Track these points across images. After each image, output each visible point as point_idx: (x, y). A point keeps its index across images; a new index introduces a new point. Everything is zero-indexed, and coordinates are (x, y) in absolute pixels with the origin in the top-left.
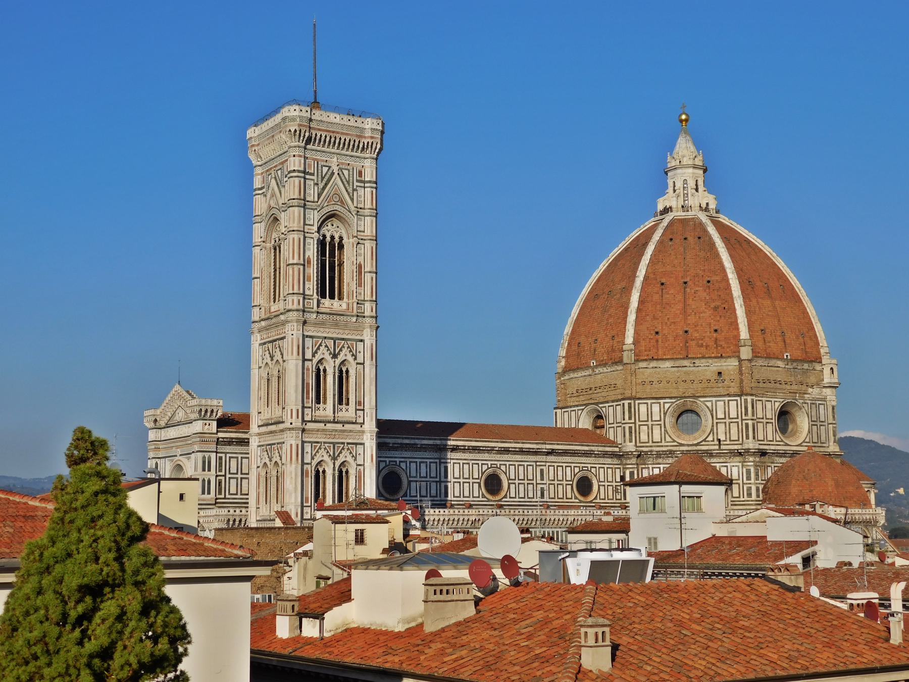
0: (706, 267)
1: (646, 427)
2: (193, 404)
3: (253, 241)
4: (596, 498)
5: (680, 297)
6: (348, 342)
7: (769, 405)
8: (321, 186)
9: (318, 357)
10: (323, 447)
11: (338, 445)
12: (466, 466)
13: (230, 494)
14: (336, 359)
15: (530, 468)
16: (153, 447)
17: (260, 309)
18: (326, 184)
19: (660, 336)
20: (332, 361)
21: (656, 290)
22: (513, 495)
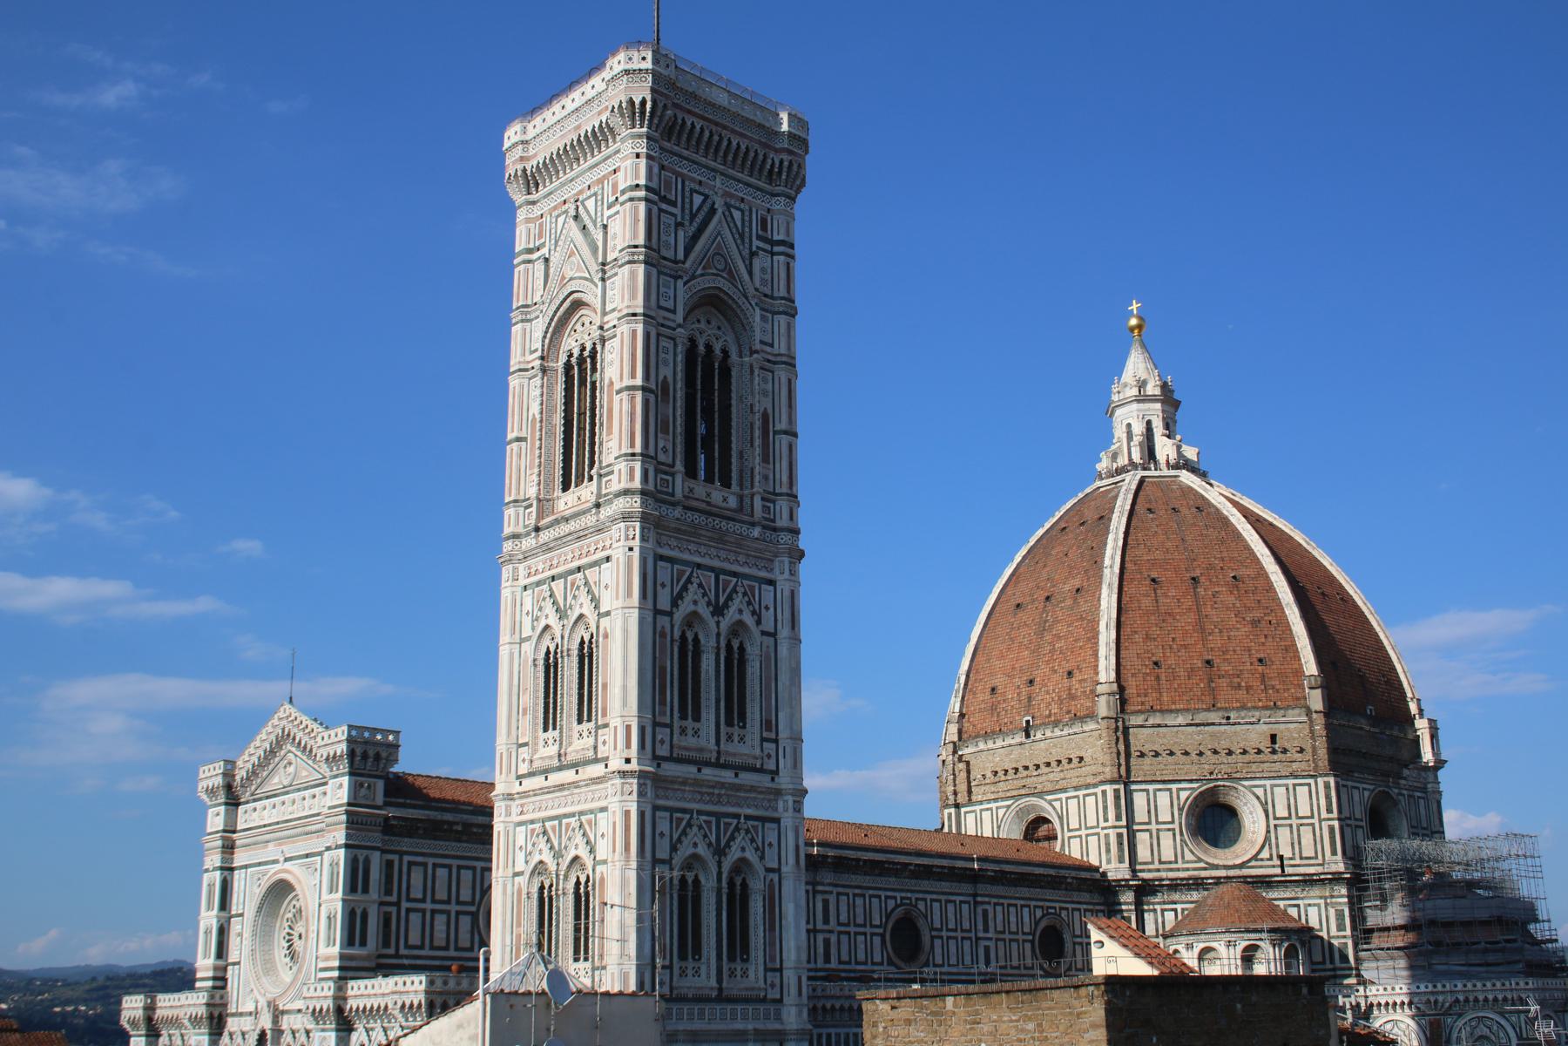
0: (1225, 554)
1: (1147, 834)
2: (334, 739)
3: (512, 363)
5: (1188, 602)
6: (745, 582)
7: (1356, 794)
9: (685, 607)
10: (692, 822)
11: (727, 820)
12: (859, 901)
13: (407, 946)
14: (721, 618)
15: (965, 907)
17: (530, 506)
19: (1163, 670)
20: (712, 622)
22: (939, 960)
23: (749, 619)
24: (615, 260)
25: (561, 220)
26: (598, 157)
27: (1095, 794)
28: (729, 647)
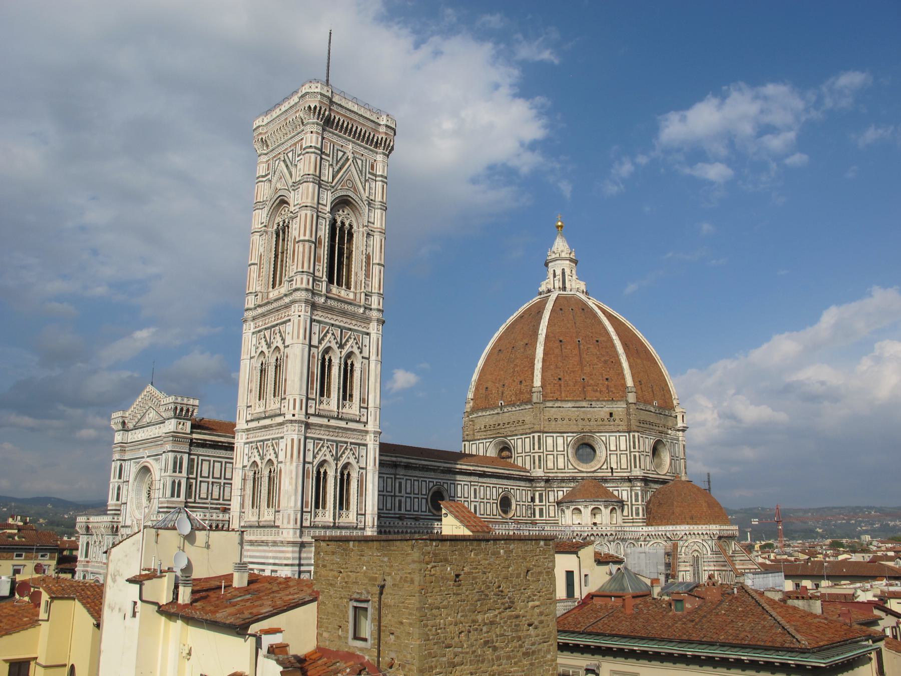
0: (593, 331)
2: (168, 402)
3: (252, 228)
4: (514, 516)
5: (576, 352)
8: (336, 169)
10: (326, 445)
11: (341, 444)
12: (416, 483)
14: (342, 350)
15: (466, 487)
16: (119, 449)
17: (257, 295)
18: (340, 169)
20: (338, 351)
21: (556, 345)
23: (357, 351)
24: (300, 181)
25: (277, 162)
26: (296, 132)
27: (530, 437)
28: (346, 364)
